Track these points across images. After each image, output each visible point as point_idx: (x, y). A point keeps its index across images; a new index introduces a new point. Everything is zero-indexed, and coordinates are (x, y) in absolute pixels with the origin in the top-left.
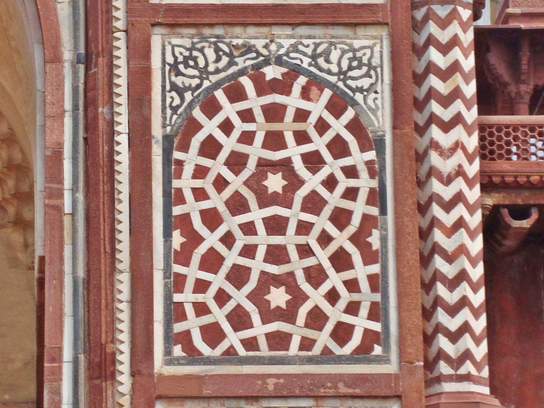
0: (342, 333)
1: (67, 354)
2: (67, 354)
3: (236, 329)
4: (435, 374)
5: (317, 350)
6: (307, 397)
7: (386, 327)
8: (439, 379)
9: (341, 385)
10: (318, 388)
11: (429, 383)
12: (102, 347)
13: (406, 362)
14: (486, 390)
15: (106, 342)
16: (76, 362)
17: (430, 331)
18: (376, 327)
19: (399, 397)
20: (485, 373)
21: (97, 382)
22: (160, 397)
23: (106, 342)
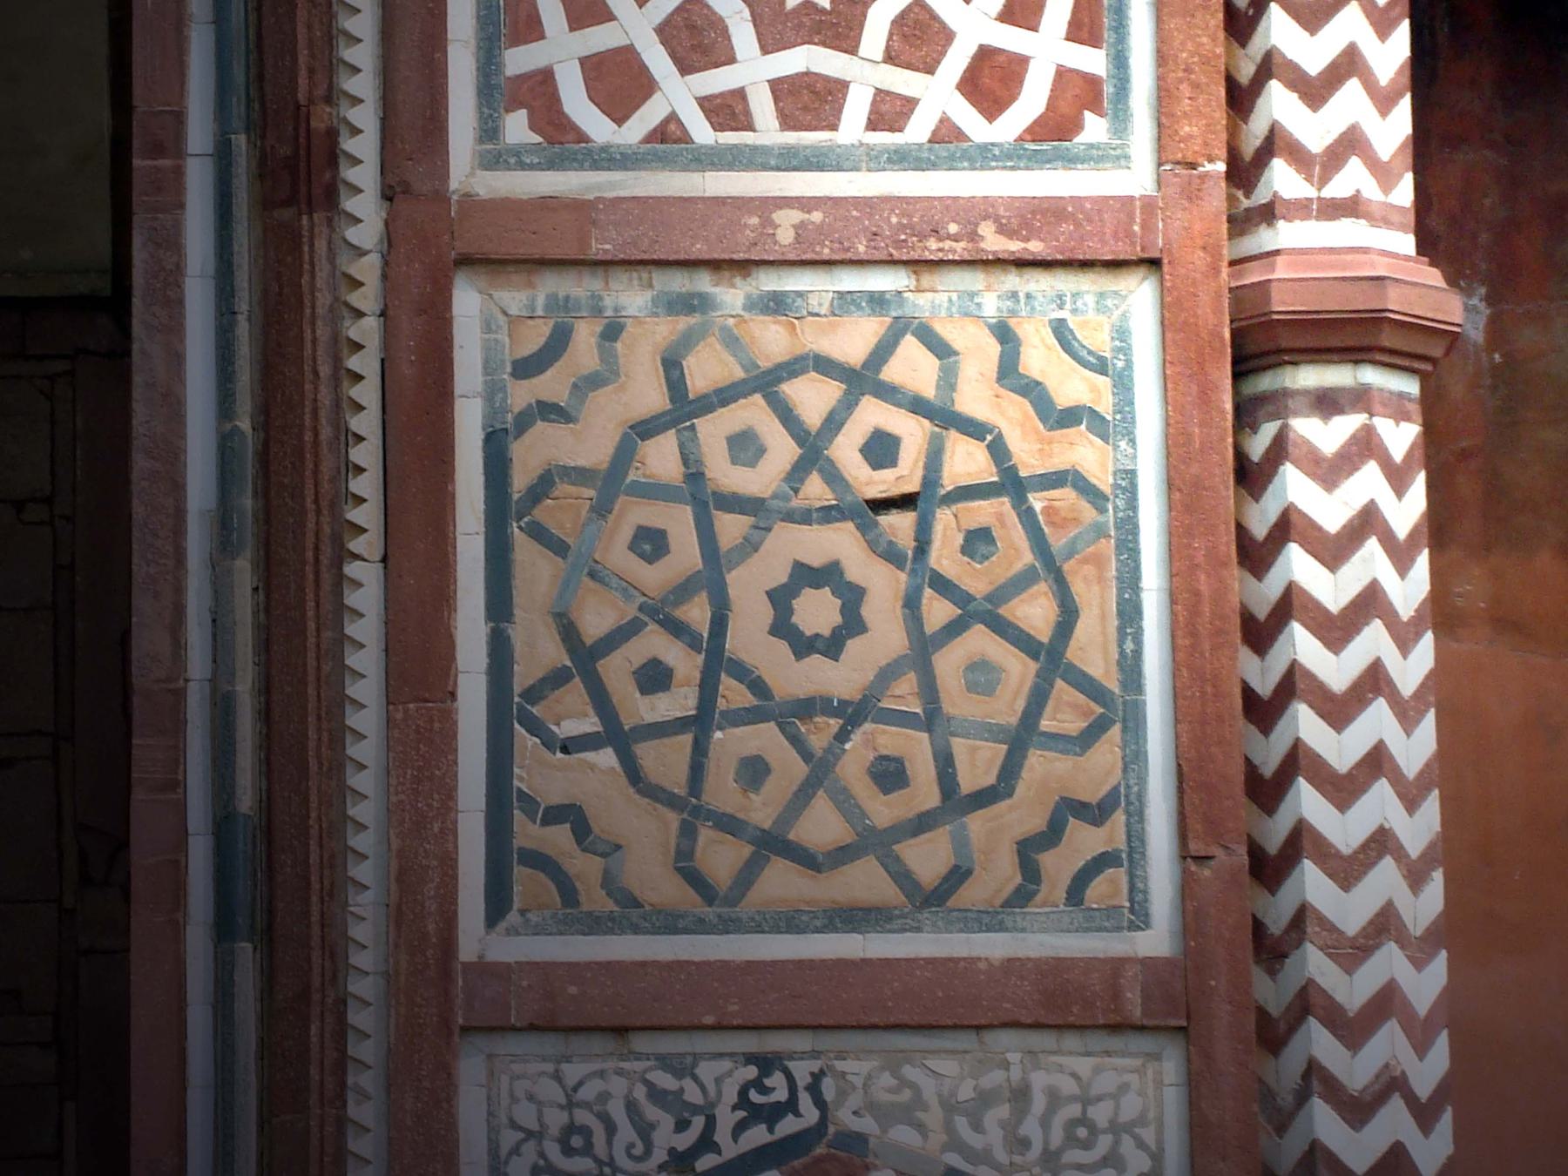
0: (991, 80)
1: (199, 133)
2: (199, 133)
3: (685, 68)
4: (1261, 196)
5: (918, 130)
6: (893, 262)
7: (1120, 61)
8: (1268, 213)
9: (986, 229)
10: (922, 237)
11: (1241, 223)
12: (300, 114)
13: (1178, 163)
14: (1407, 243)
15: (311, 101)
16: (223, 155)
17: (1246, 72)
18: (1093, 61)
19: (1154, 263)
20: (1404, 193)
21: (286, 214)
22: (466, 261)
23: (311, 101)
